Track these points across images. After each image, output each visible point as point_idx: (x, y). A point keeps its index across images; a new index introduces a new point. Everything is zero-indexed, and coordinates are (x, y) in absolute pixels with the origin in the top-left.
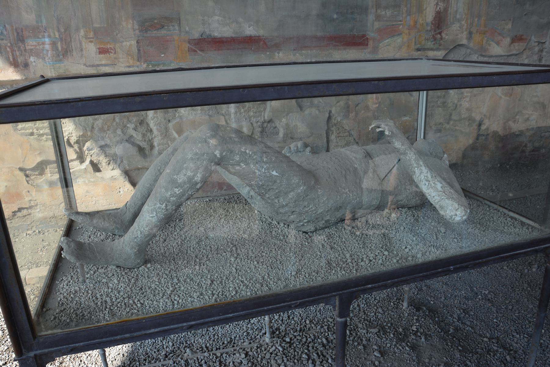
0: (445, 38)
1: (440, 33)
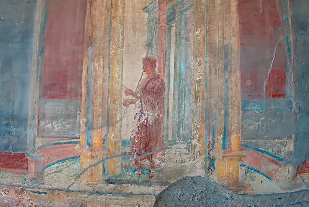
0: (159, 166)
1: (150, 158)
